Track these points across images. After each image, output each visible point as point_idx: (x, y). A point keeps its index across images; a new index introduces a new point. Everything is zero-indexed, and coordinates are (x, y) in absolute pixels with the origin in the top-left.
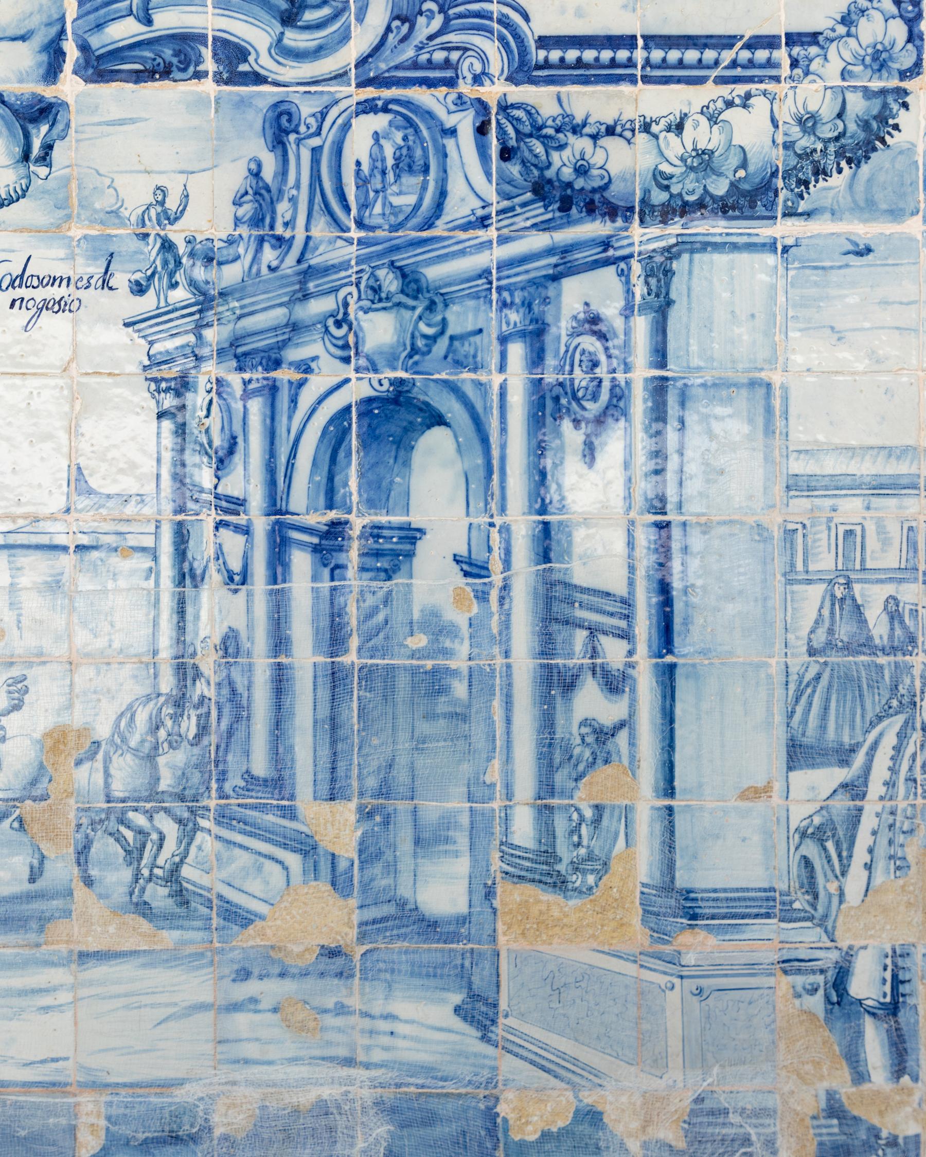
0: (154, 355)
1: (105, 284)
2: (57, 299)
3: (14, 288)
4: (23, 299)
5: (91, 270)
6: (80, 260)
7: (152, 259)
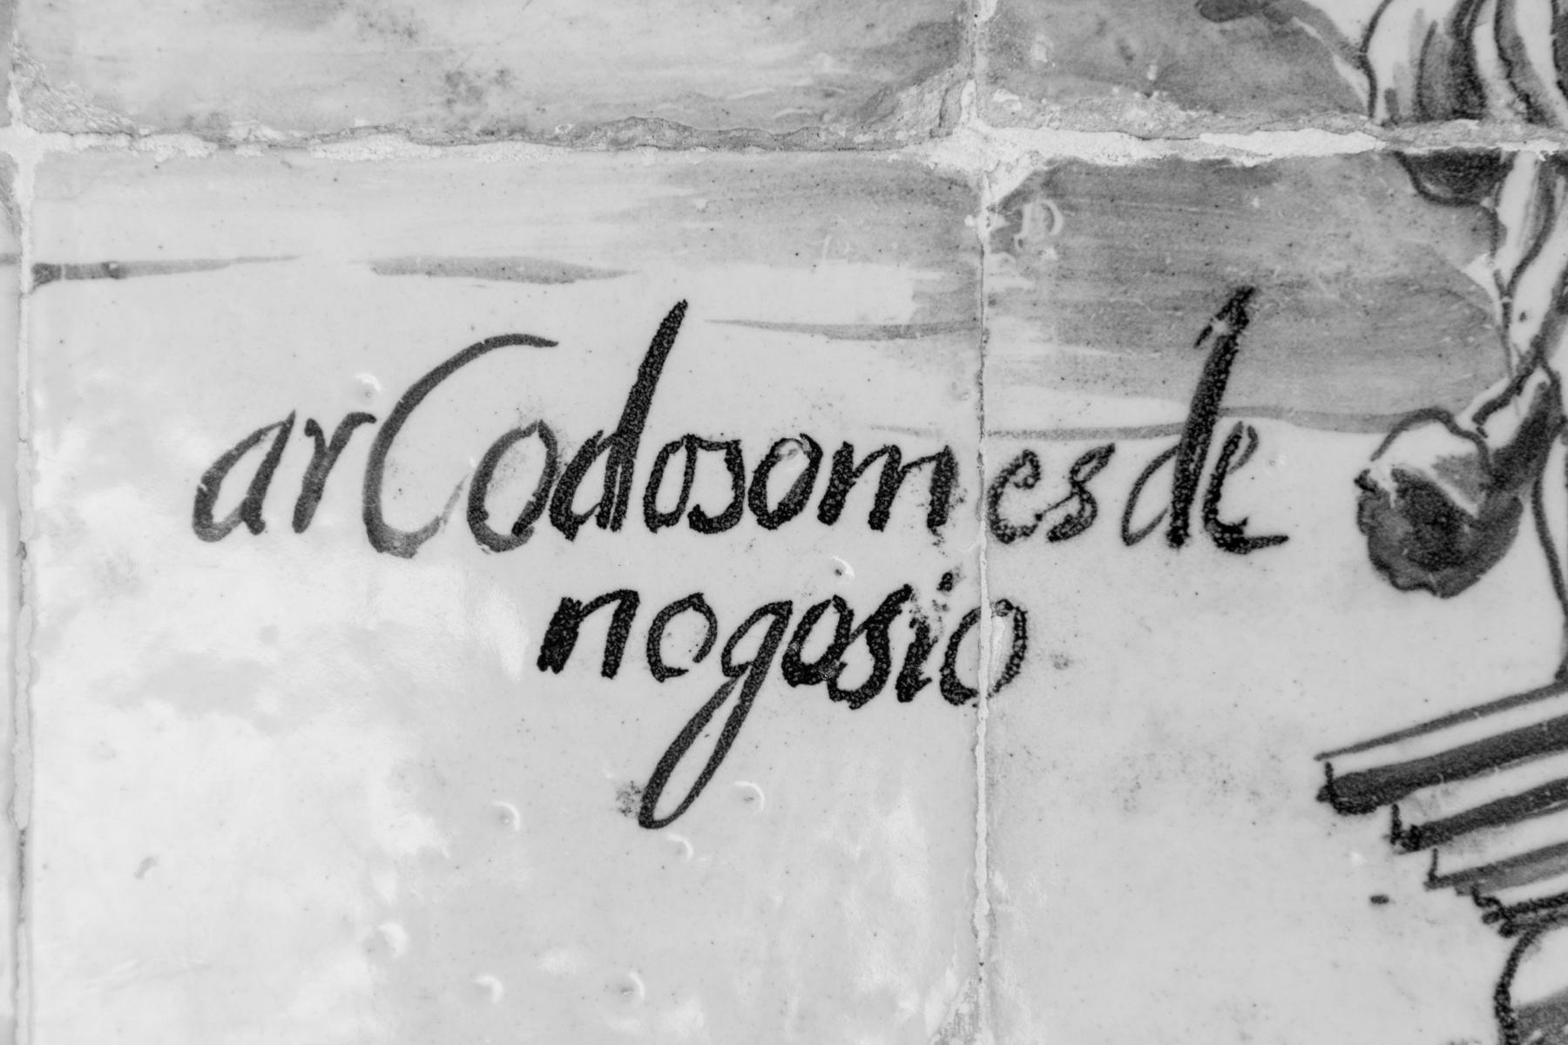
0: (1534, 1013)
1: (1197, 495)
2: (864, 608)
3: (568, 525)
4: (628, 601)
5: (1108, 411)
6: (1020, 341)
7: (1522, 335)
